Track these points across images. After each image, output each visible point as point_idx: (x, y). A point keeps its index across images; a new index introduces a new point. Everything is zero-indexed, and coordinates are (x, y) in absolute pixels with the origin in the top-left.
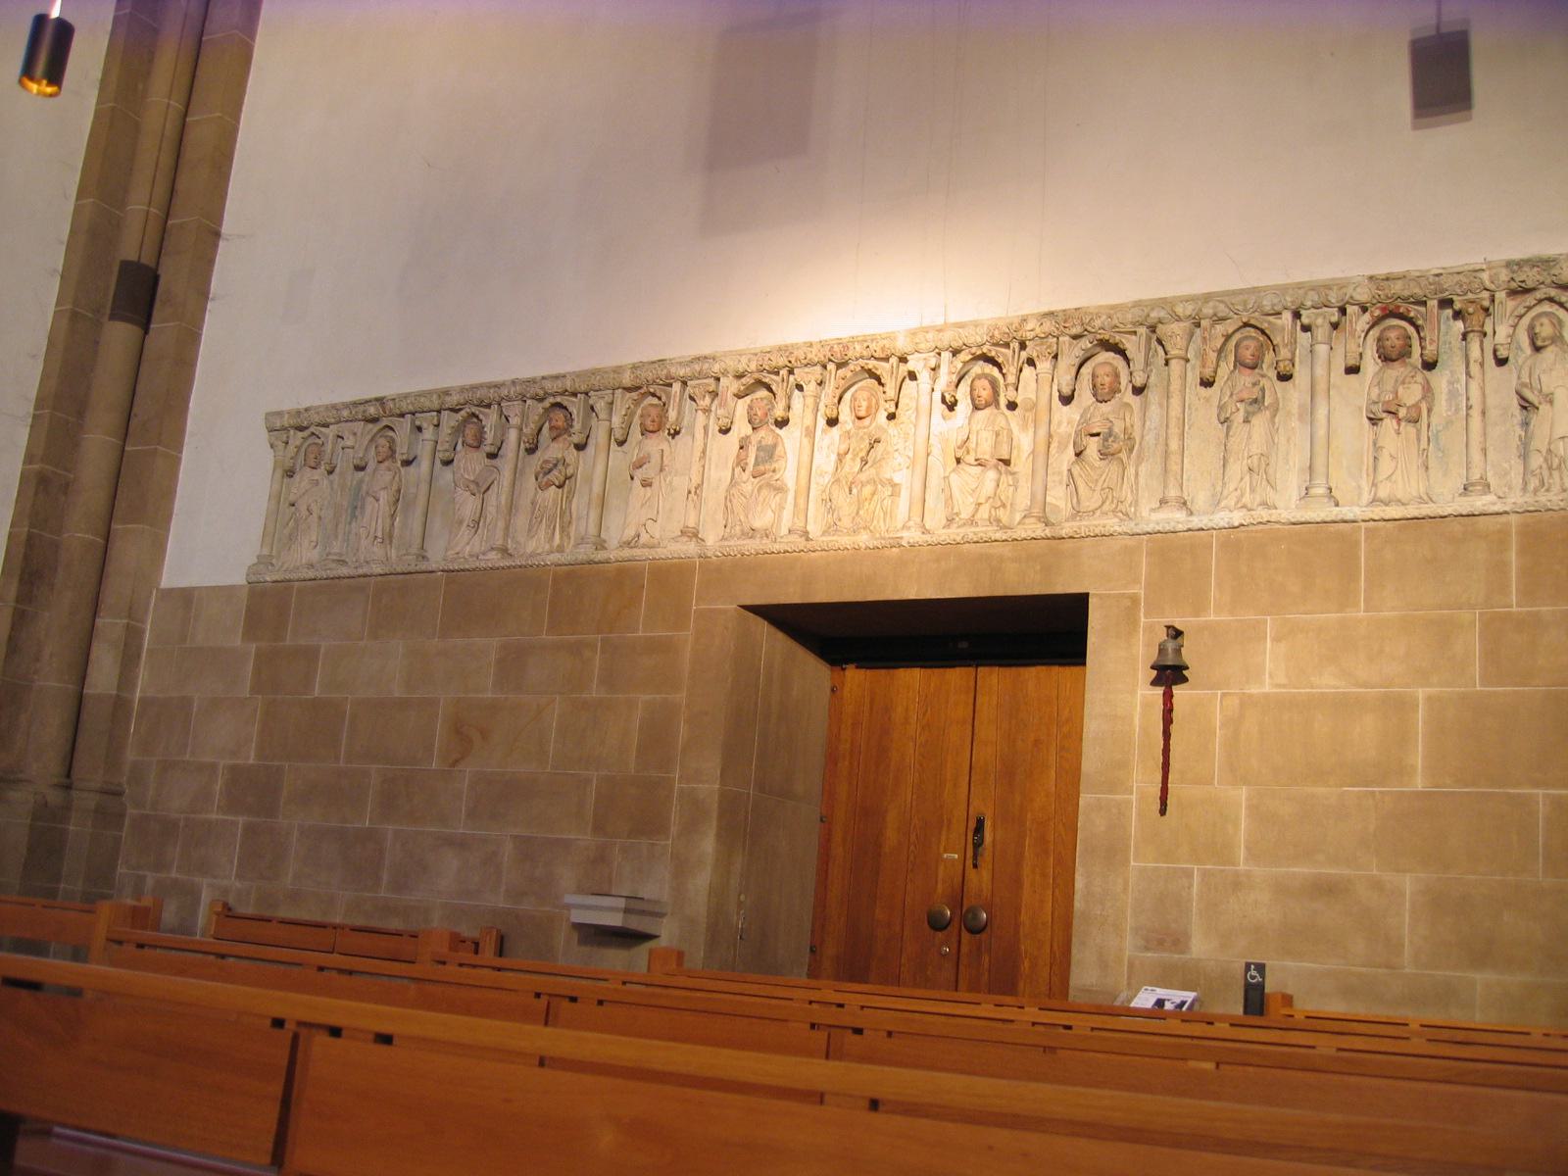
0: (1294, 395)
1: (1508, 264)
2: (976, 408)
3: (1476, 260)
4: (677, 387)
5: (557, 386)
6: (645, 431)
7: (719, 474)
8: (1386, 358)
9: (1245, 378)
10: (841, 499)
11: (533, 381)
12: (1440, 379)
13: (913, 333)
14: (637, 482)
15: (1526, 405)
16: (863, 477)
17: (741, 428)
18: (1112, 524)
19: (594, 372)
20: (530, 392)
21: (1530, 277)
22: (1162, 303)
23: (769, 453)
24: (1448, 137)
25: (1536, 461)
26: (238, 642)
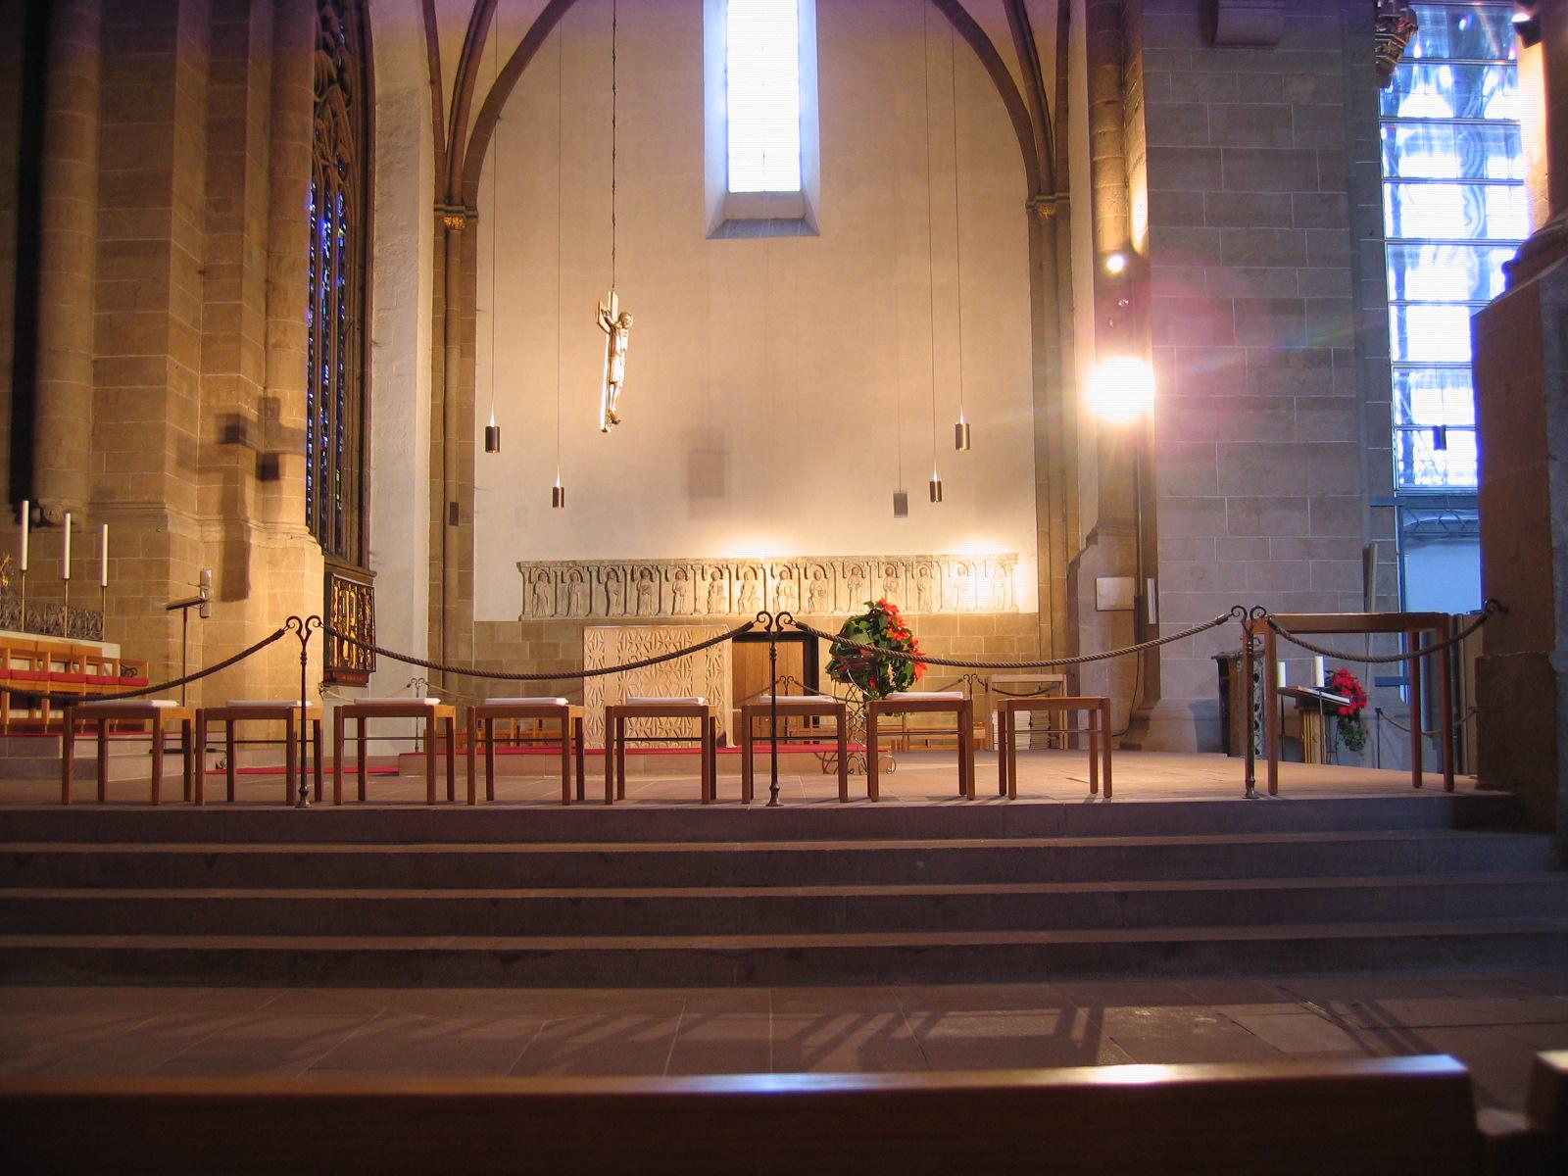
0: (866, 582)
1: (917, 556)
2: (782, 578)
3: (908, 554)
4: (689, 567)
5: (647, 563)
6: (677, 577)
7: (703, 593)
8: (888, 575)
9: (855, 578)
10: (746, 603)
11: (637, 561)
12: (900, 581)
13: (766, 559)
14: (678, 595)
15: (919, 589)
16: (753, 597)
17: (709, 580)
18: (824, 614)
19: (660, 560)
20: (634, 563)
21: (921, 559)
22: (835, 557)
23: (720, 589)
24: (902, 521)
25: (922, 603)
26: (521, 641)
